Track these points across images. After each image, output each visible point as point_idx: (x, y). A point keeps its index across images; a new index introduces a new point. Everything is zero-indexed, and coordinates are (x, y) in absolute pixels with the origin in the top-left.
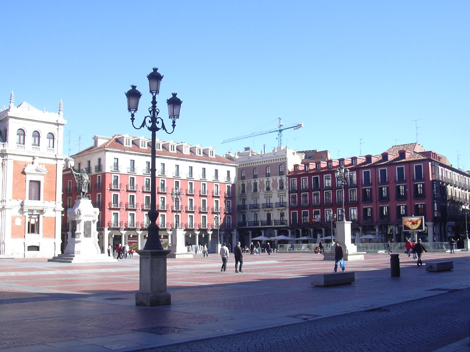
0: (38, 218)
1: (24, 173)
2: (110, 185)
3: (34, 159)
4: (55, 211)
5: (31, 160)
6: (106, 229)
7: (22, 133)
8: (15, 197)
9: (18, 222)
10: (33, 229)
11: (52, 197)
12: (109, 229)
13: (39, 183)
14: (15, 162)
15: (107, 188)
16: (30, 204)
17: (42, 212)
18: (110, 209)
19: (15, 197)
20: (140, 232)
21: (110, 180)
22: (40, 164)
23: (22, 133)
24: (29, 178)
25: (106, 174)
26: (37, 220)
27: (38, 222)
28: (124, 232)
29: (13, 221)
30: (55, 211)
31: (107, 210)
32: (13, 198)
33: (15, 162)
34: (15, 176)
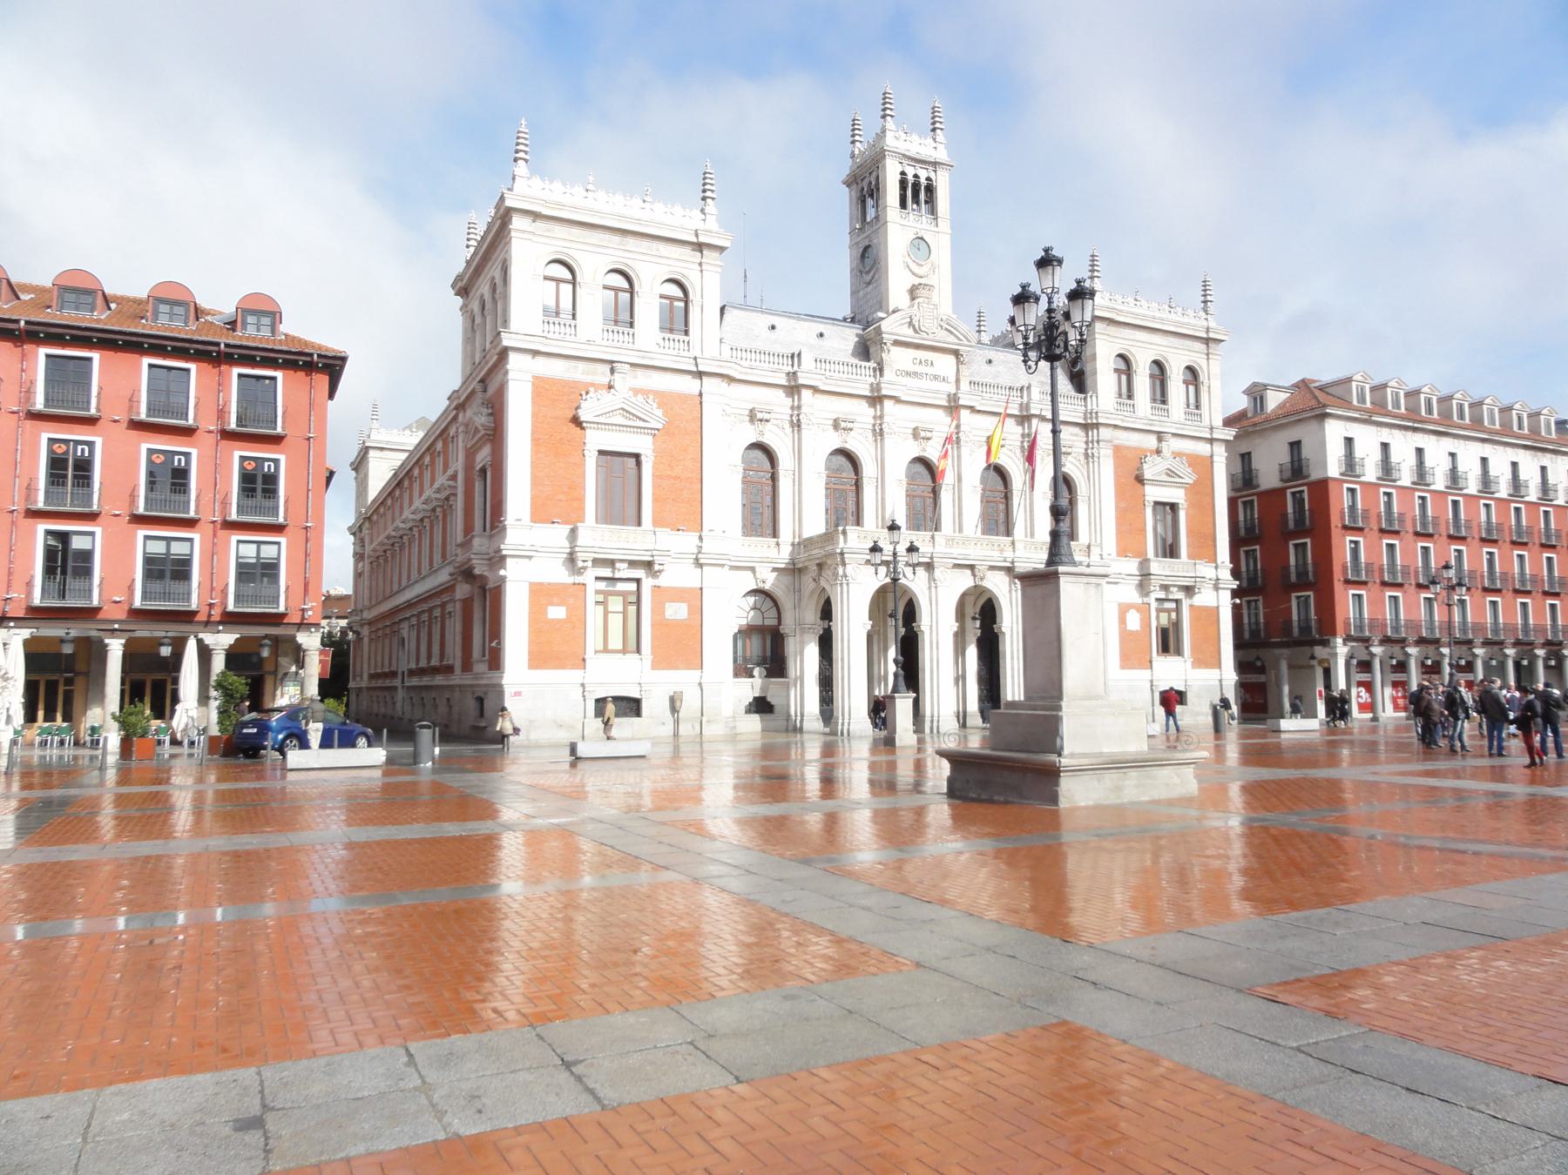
0: (1178, 610)
1: (1140, 480)
2: (1343, 518)
3: (1160, 440)
4: (701, 566)
5: (1151, 442)
6: (1339, 641)
7: (1125, 364)
8: (1123, 552)
9: (1134, 622)
10: (1168, 642)
11: (1204, 548)
12: (1345, 641)
13: (1173, 507)
14: (1118, 450)
15: (1335, 521)
16: (1160, 568)
17: (1189, 590)
18: (1347, 582)
19: (1123, 552)
20: (1412, 651)
21: (1340, 502)
22: (1176, 455)
23: (1125, 364)
24: (1153, 493)
25: (1331, 486)
26: (1174, 615)
27: (1177, 625)
28: (1377, 650)
29: (1122, 621)
30: (701, 566)
31: (1338, 586)
32: (1119, 554)
33: (1118, 450)
34: (1120, 493)
